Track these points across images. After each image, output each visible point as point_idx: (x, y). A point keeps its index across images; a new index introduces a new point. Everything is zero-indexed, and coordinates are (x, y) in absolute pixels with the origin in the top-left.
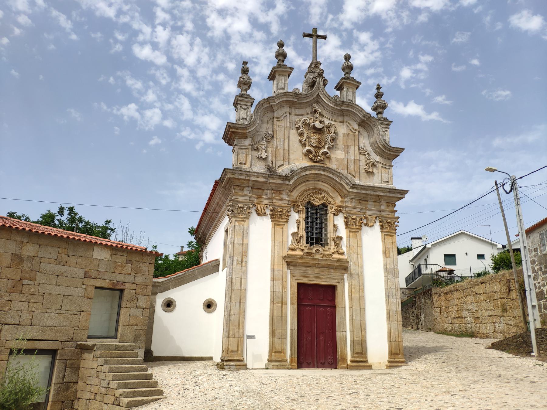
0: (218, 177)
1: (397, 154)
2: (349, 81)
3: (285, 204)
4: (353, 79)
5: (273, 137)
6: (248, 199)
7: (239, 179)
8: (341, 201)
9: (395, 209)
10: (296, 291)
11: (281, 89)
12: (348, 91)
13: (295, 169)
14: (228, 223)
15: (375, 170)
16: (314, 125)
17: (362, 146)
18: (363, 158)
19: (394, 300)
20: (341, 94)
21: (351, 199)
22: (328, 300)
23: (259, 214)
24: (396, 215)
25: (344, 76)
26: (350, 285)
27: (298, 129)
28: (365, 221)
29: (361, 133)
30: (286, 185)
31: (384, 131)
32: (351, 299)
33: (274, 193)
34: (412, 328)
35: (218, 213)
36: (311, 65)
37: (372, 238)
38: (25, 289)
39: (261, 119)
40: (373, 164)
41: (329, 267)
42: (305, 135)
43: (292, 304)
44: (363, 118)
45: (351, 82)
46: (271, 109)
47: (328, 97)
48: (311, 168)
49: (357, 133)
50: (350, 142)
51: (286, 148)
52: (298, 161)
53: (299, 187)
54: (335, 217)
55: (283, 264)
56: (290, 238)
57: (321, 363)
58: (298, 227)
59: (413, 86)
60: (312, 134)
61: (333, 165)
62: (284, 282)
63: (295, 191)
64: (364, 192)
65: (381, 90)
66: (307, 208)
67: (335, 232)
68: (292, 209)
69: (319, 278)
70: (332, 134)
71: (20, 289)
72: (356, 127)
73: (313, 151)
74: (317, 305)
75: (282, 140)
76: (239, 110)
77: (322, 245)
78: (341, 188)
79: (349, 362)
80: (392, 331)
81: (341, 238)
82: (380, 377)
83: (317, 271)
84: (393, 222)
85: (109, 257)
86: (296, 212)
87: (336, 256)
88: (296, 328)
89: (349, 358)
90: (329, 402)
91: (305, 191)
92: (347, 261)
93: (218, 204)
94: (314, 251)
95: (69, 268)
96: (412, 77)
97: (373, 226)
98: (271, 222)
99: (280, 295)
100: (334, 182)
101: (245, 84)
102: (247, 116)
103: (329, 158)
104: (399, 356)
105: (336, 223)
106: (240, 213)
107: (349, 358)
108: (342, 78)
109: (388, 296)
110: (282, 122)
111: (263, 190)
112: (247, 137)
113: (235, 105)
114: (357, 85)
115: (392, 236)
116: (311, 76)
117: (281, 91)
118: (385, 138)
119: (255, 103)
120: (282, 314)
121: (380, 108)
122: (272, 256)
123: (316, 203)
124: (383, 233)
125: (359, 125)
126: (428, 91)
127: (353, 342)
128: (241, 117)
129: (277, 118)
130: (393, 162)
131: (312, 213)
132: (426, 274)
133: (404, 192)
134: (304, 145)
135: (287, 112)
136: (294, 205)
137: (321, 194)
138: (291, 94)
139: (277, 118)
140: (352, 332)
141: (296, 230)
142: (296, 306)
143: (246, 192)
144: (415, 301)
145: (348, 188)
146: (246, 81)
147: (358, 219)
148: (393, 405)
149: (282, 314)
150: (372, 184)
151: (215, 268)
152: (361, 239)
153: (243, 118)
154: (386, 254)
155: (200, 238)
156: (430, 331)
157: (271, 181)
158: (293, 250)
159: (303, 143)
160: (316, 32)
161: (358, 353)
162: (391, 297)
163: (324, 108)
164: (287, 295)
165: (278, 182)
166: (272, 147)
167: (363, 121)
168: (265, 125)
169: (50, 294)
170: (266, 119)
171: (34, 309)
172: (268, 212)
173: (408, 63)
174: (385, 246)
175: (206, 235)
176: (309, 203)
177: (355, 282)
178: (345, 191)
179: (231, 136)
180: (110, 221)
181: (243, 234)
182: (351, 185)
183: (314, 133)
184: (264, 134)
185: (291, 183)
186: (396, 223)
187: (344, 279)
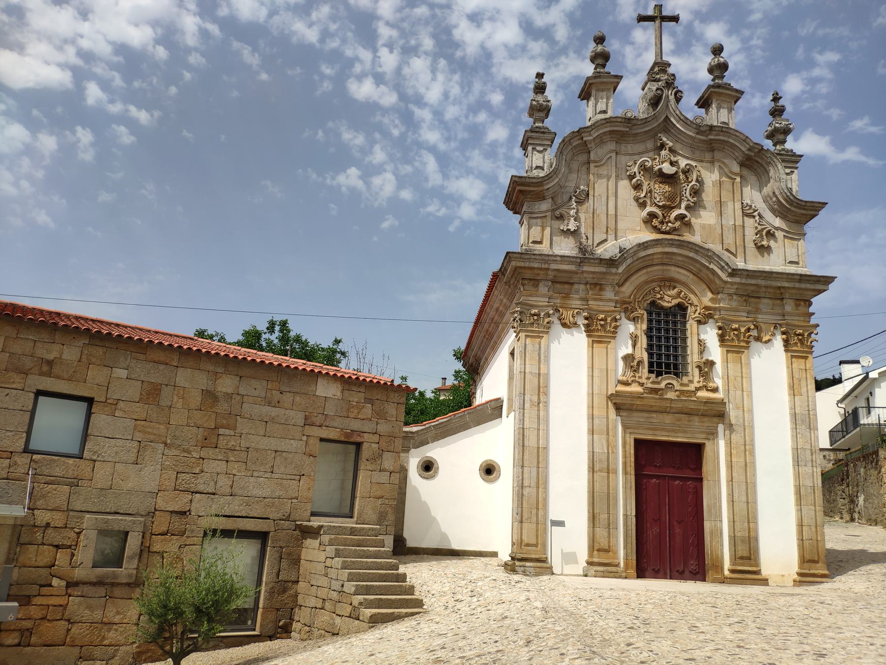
0: (496, 267)
1: (812, 213)
2: (721, 90)
3: (610, 306)
4: (728, 87)
5: (588, 195)
6: (547, 300)
7: (532, 268)
8: (712, 300)
9: (811, 310)
10: (632, 452)
11: (601, 112)
12: (719, 108)
13: (628, 246)
14: (514, 341)
15: (772, 243)
16: (660, 170)
17: (747, 201)
18: (749, 222)
19: (808, 469)
20: (707, 113)
21: (730, 295)
22: (690, 468)
23: (564, 325)
24: (813, 321)
25: (712, 83)
26: (729, 444)
27: (631, 177)
28: (754, 333)
30: (612, 274)
31: (787, 174)
32: (730, 466)
33: (591, 289)
34: (842, 518)
35: (497, 325)
36: (652, 68)
37: (770, 362)
38: (222, 442)
39: (568, 166)
40: (768, 233)
41: (690, 413)
42: (645, 188)
43: (625, 472)
45: (725, 91)
46: (585, 148)
47: (685, 121)
48: (656, 242)
49: (738, 179)
50: (726, 195)
51: (612, 211)
52: (634, 233)
53: (636, 276)
54: (701, 327)
55: (607, 408)
56: (621, 364)
57: (678, 571)
58: (634, 346)
59: (806, 106)
60: (656, 186)
61: (696, 239)
62: (611, 438)
63: (628, 284)
64: (753, 282)
65: (781, 102)
66: (650, 313)
67: (701, 352)
68: (623, 315)
69: (673, 431)
70: (694, 183)
71: (215, 441)
72: (736, 168)
73: (660, 213)
74: (669, 477)
75: (604, 199)
76: (530, 155)
77: (677, 375)
78: (711, 276)
79: (726, 573)
80: (805, 522)
81: (712, 364)
82: (782, 600)
83: (668, 419)
84: (806, 334)
85: (339, 394)
86: (629, 319)
87: (702, 394)
88: (634, 513)
89: (727, 565)
90: (693, 636)
91: (646, 282)
92: (722, 403)
93: (497, 310)
94: (663, 385)
95: (282, 411)
96: (803, 92)
97: (769, 340)
98: (586, 339)
99: (604, 457)
100: (697, 265)
101: (541, 110)
102: (544, 162)
103: (688, 225)
104: (821, 564)
105: (702, 337)
106: (534, 325)
107: (727, 565)
108: (710, 87)
109: (797, 462)
110: (605, 167)
111: (572, 284)
112: (544, 198)
113: (524, 146)
114: (738, 95)
115: (806, 358)
116: (654, 86)
117: (602, 116)
118: (789, 186)
119: (558, 141)
120: (609, 489)
121: (779, 134)
122: (588, 394)
123: (665, 304)
124: (789, 354)
126: (835, 113)
127: (733, 539)
128: (534, 166)
129: (595, 162)
130: (805, 227)
131: (659, 322)
132: (868, 424)
133: (827, 280)
134: (643, 205)
136: (627, 308)
137: (674, 288)
138: (619, 120)
139: (595, 162)
140: (733, 522)
141: (630, 351)
142: (633, 477)
143: (543, 289)
144: (848, 471)
145: (724, 276)
147: (743, 330)
148: (807, 648)
149: (609, 489)
150: (767, 268)
151: (496, 412)
152: (749, 364)
153: (537, 167)
154: (793, 389)
155: (472, 365)
156: (876, 525)
157: (585, 268)
158: (626, 384)
159: (641, 201)
160: (661, 12)
161: (742, 558)
162: (803, 464)
163: (676, 140)
164: (616, 459)
165: (597, 269)
166: (587, 212)
167: (749, 158)
168: (574, 176)
169: (257, 450)
170: (575, 166)
171: (234, 472)
172: (581, 321)
173: (795, 67)
174: (792, 376)
175: (481, 359)
176: (653, 303)
177: (736, 438)
178: (717, 281)
179: (517, 198)
180: (340, 341)
181: (540, 358)
182: (730, 270)
183: (660, 183)
184: (572, 189)
185: (620, 270)
186: (813, 335)
187: (717, 433)
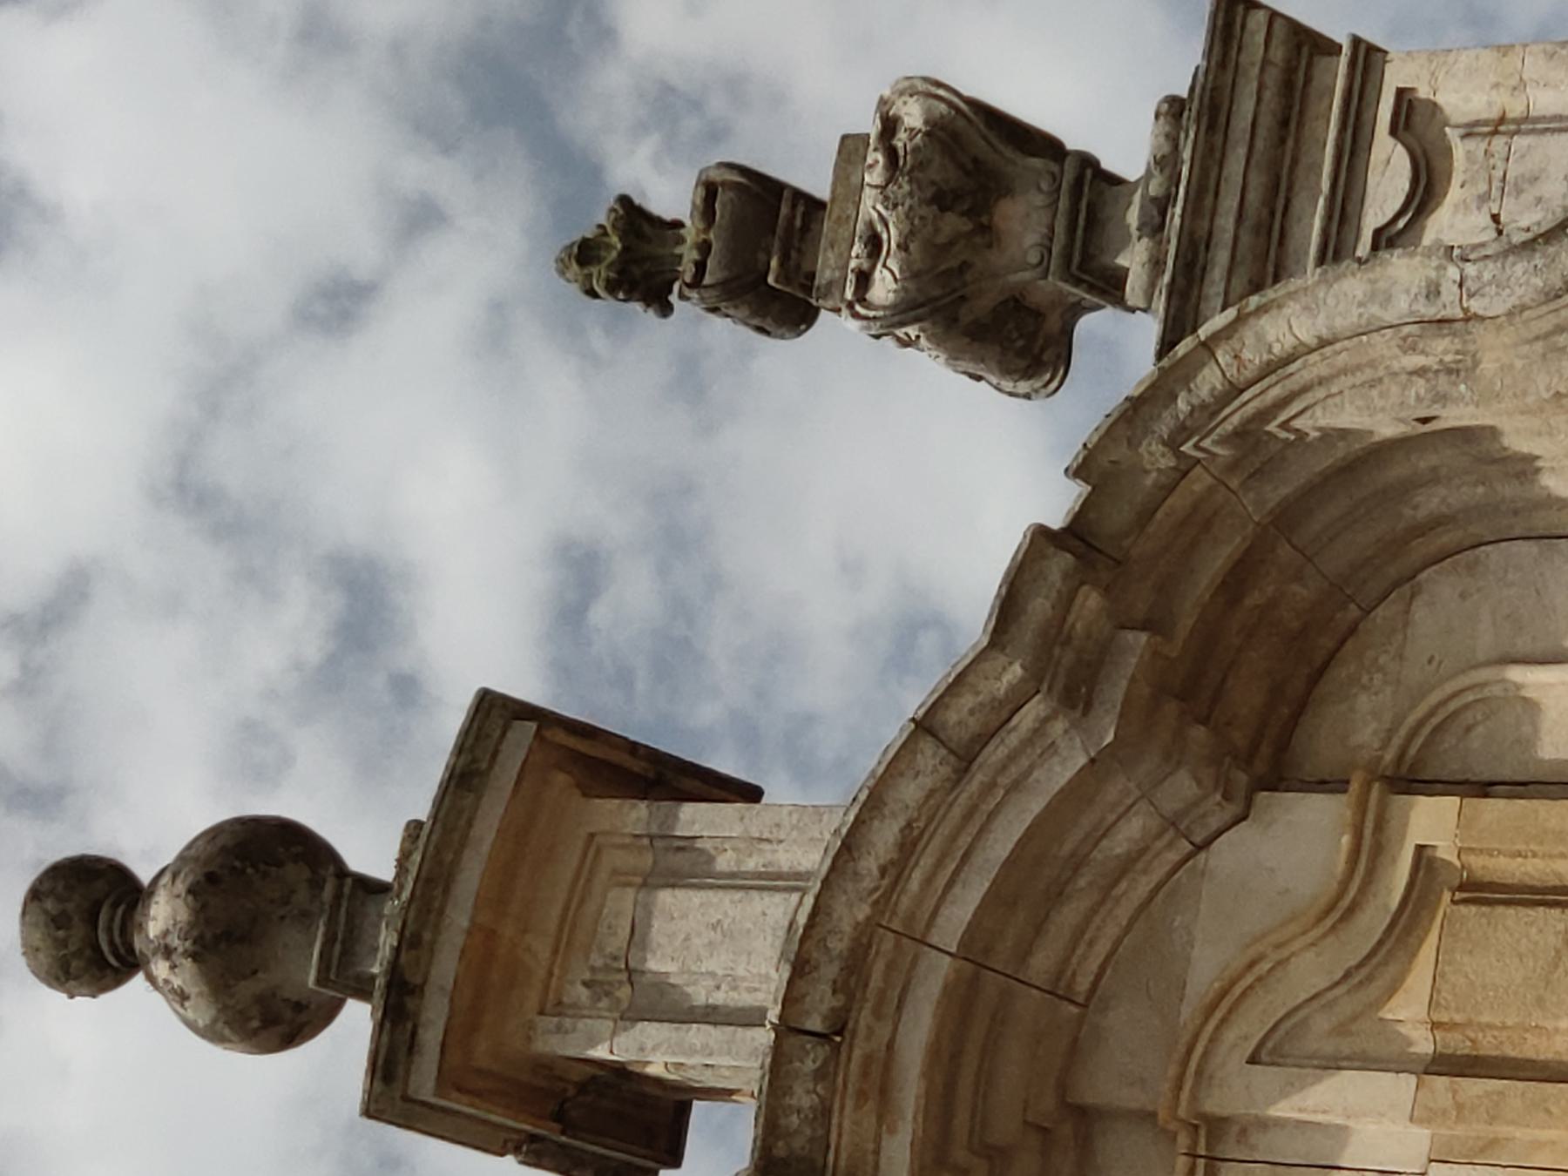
29: (1444, 723)
44: (1114, 690)
72: (1299, 839)
125: (1270, 763)
167: (1188, 689)
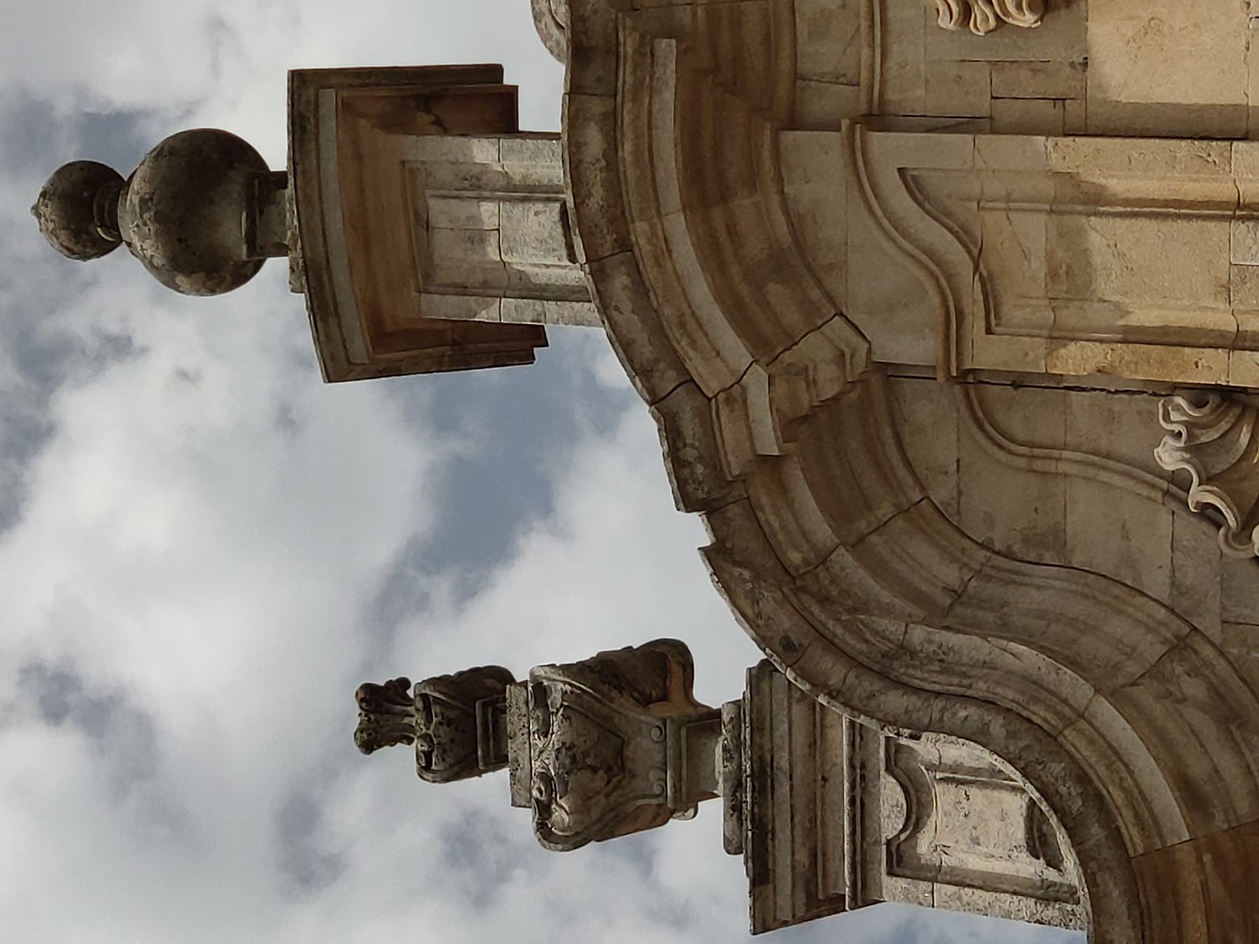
46: (854, 425)
110: (993, 226)
128: (1029, 868)
129: (952, 324)
135: (858, 163)
146: (572, 756)
170: (999, 499)
